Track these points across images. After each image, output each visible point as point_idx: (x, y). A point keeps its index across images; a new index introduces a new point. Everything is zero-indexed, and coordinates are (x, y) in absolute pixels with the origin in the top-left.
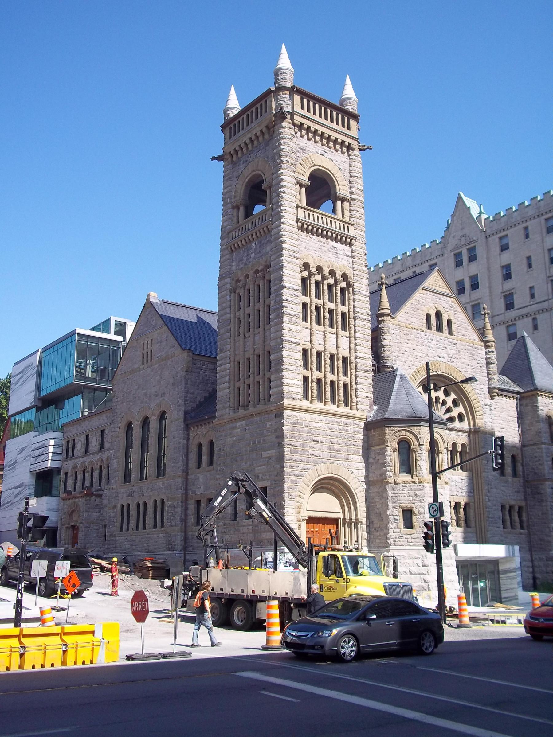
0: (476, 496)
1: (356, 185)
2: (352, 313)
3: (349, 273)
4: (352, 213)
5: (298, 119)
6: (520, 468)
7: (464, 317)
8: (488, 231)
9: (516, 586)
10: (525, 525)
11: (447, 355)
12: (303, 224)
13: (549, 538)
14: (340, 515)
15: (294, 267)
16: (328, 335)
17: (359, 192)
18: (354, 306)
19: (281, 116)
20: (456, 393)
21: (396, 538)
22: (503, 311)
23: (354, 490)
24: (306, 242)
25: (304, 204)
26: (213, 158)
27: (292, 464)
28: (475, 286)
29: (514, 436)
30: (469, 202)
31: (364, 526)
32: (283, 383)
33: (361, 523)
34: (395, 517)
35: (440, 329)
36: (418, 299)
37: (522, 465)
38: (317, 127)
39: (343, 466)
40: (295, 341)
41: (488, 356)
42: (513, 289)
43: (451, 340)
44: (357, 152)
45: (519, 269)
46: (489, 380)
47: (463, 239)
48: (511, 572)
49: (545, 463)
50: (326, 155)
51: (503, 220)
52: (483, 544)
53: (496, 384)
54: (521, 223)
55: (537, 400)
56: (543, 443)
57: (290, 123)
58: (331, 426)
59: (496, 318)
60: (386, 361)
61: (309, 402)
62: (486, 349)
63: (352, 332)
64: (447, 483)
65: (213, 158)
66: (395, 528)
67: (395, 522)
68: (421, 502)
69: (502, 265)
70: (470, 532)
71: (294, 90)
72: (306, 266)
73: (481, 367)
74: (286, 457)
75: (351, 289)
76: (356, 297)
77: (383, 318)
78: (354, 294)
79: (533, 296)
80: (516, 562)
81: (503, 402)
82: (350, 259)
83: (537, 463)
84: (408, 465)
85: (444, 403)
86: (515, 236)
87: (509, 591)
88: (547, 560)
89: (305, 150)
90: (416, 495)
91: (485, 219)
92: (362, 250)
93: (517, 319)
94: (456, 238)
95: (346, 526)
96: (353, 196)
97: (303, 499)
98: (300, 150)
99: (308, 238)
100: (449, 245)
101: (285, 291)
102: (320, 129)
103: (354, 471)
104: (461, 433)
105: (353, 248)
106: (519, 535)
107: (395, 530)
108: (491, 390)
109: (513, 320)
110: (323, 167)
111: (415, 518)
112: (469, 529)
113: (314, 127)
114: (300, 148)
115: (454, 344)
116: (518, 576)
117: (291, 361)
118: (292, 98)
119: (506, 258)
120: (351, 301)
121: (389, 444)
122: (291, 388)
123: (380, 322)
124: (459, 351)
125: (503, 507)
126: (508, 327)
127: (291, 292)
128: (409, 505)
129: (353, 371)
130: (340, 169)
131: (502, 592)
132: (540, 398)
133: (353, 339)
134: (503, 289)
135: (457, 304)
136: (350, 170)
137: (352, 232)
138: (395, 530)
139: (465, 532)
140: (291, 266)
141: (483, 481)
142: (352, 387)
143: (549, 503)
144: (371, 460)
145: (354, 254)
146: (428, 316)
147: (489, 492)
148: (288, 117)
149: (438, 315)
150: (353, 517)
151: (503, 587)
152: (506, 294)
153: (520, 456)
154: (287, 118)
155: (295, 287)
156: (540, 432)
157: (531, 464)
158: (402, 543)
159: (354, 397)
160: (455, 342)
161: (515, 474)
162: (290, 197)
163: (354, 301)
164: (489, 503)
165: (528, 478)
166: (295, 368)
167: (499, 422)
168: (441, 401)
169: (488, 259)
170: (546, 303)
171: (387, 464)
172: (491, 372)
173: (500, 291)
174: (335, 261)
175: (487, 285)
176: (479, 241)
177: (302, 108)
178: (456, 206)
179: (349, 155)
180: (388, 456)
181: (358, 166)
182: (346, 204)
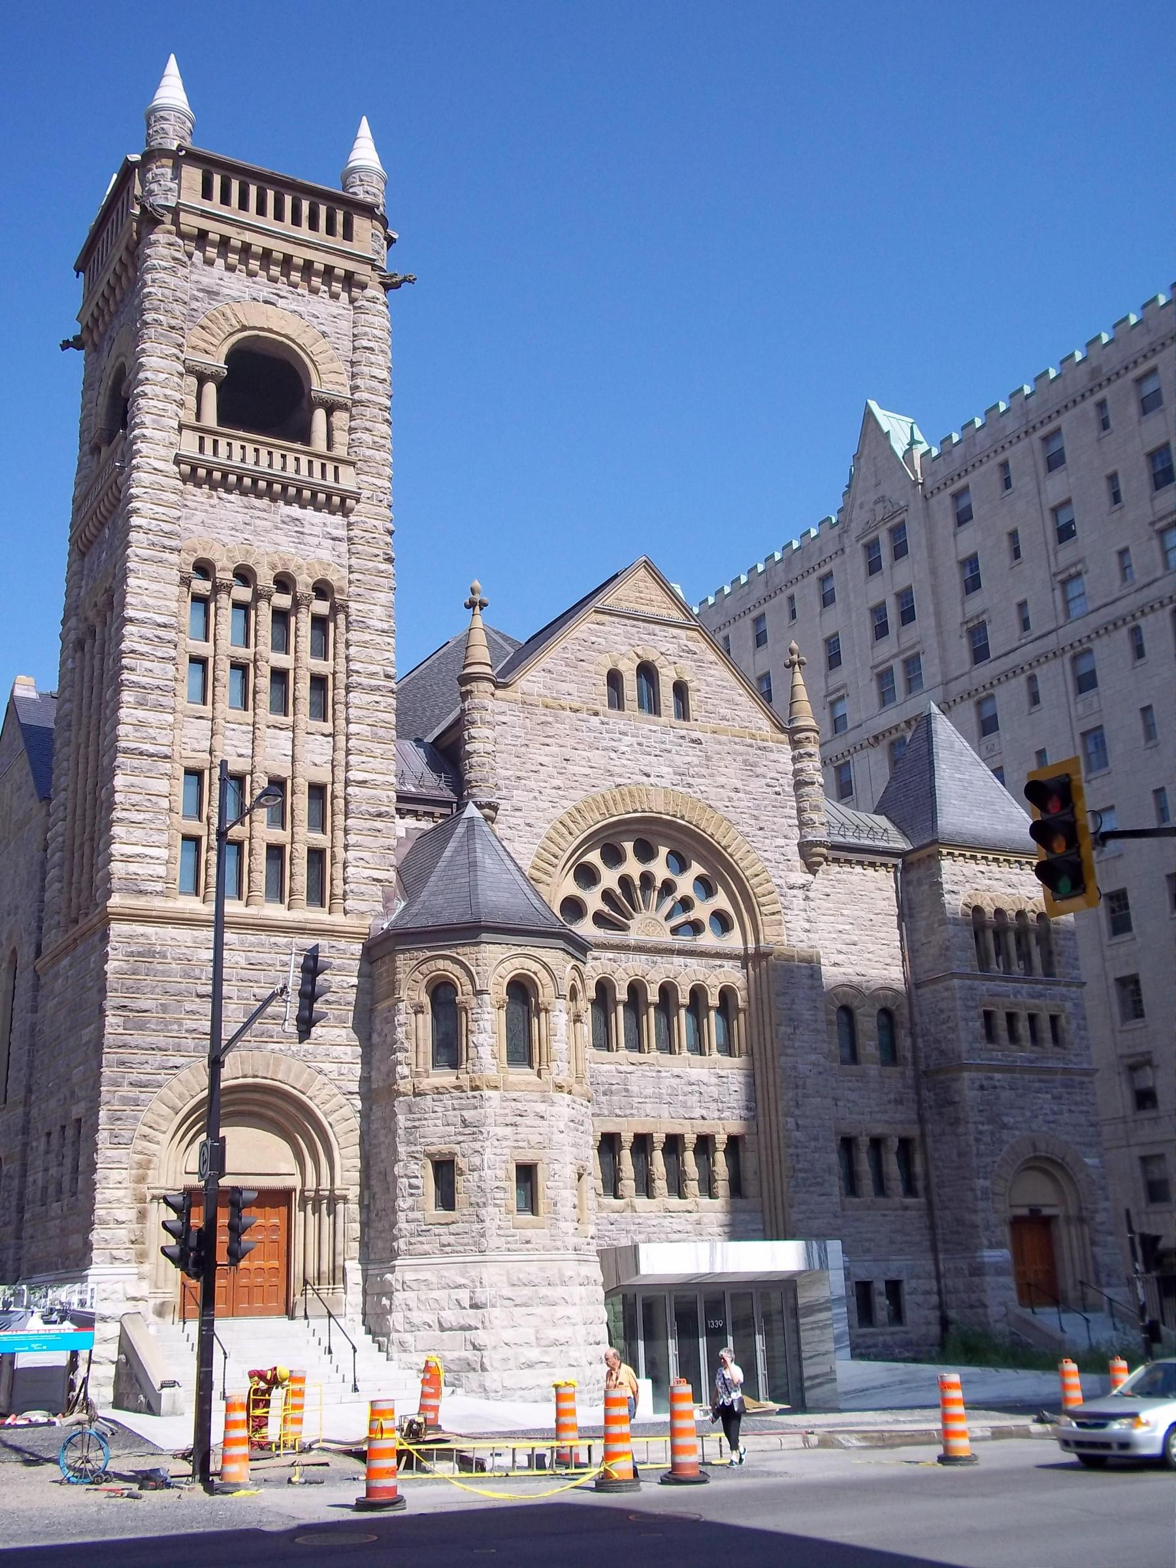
0: (761, 1118)
1: (366, 370)
2: (341, 677)
3: (335, 578)
4: (353, 436)
5: (190, 222)
6: (904, 1042)
7: (727, 675)
8: (929, 483)
9: (831, 1346)
10: (920, 1185)
11: (670, 770)
12: (194, 469)
13: (974, 1217)
14: (295, 1182)
15: (162, 571)
16: (265, 733)
17: (375, 384)
18: (348, 659)
19: (150, 220)
20: (703, 861)
21: (412, 1235)
22: (967, 667)
23: (326, 1115)
24: (206, 511)
25: (210, 418)
26: (66, 345)
27: (125, 1057)
28: (908, 616)
29: (889, 961)
30: (887, 420)
31: (354, 1208)
32: (111, 855)
33: (345, 1199)
34: (413, 1181)
35: (651, 705)
36: (584, 636)
37: (912, 1034)
38: (248, 237)
39: (293, 1056)
40: (152, 749)
41: (799, 766)
42: (983, 613)
43: (683, 732)
44: (375, 291)
45: (994, 563)
46: (802, 824)
47: (880, 505)
48: (820, 1311)
49: (961, 1024)
50: (281, 302)
51: (957, 452)
52: (778, 1239)
53: (819, 834)
54: (992, 455)
55: (940, 869)
56: (954, 975)
57: (169, 232)
58: (255, 957)
59: (952, 685)
60: (475, 790)
61: (200, 899)
62: (794, 749)
63: (341, 723)
64: (560, 1088)
65: (66, 345)
66: (412, 1209)
67: (412, 1195)
68: (475, 1140)
69: (961, 557)
70: (744, 1211)
71: (183, 158)
72: (204, 569)
73: (778, 794)
74: (109, 1039)
75: (341, 617)
76: (353, 636)
77: (468, 687)
78: (348, 630)
79: (1025, 624)
80: (835, 1283)
81: (854, 878)
82: (343, 547)
83: (944, 1027)
84: (449, 1048)
85: (668, 887)
86: (982, 484)
87: (816, 1360)
88: (971, 1275)
89: (217, 294)
90: (464, 1121)
91: (922, 456)
92: (376, 523)
93: (995, 682)
94: (866, 507)
95: (309, 1207)
96: (356, 396)
97: (158, 1143)
98: (201, 295)
99: (215, 501)
100: (853, 525)
101: (129, 629)
102: (259, 242)
103: (326, 1067)
104: (718, 962)
105: (352, 519)
106: (900, 1212)
107: (411, 1215)
108: (805, 848)
109: (988, 686)
110: (270, 330)
111: (460, 1182)
112: (740, 1203)
113: (238, 237)
114: (199, 290)
115: (693, 741)
116: (838, 1321)
117: (136, 798)
118: (177, 176)
119: (969, 540)
120: (341, 647)
121: (403, 994)
122: (133, 868)
123: (465, 696)
124: (708, 758)
125: (848, 1144)
126: (979, 704)
127: (148, 632)
128: (444, 1148)
129: (340, 819)
130: (324, 335)
131: (804, 1363)
132: (946, 864)
133: (341, 739)
134: (964, 614)
135: (704, 645)
136: (355, 335)
137: (348, 479)
138: (411, 1215)
139: (733, 1211)
140: (151, 568)
141: (778, 1080)
142: (333, 857)
143: (971, 1126)
144: (376, 1038)
145: (352, 533)
146: (614, 679)
147: (798, 1105)
148: (168, 218)
149: (647, 671)
150: (325, 1184)
151: (807, 1351)
152: (971, 625)
153: (906, 1011)
154: (163, 223)
155: (161, 619)
156: (947, 948)
157: (933, 1030)
158: (426, 1247)
159: (339, 882)
160: (696, 735)
161: (890, 1055)
162: (160, 405)
163: (348, 645)
164: (798, 1134)
165: (928, 1066)
166: (148, 816)
167: (841, 927)
168: (658, 884)
169: (931, 548)
170: (1053, 636)
171: (398, 1045)
172: (806, 805)
173: (960, 620)
174: (293, 551)
175: (931, 609)
176: (912, 509)
177: (207, 194)
178: (863, 435)
179: (352, 301)
180: (400, 1025)
181: (378, 320)
182: (340, 418)
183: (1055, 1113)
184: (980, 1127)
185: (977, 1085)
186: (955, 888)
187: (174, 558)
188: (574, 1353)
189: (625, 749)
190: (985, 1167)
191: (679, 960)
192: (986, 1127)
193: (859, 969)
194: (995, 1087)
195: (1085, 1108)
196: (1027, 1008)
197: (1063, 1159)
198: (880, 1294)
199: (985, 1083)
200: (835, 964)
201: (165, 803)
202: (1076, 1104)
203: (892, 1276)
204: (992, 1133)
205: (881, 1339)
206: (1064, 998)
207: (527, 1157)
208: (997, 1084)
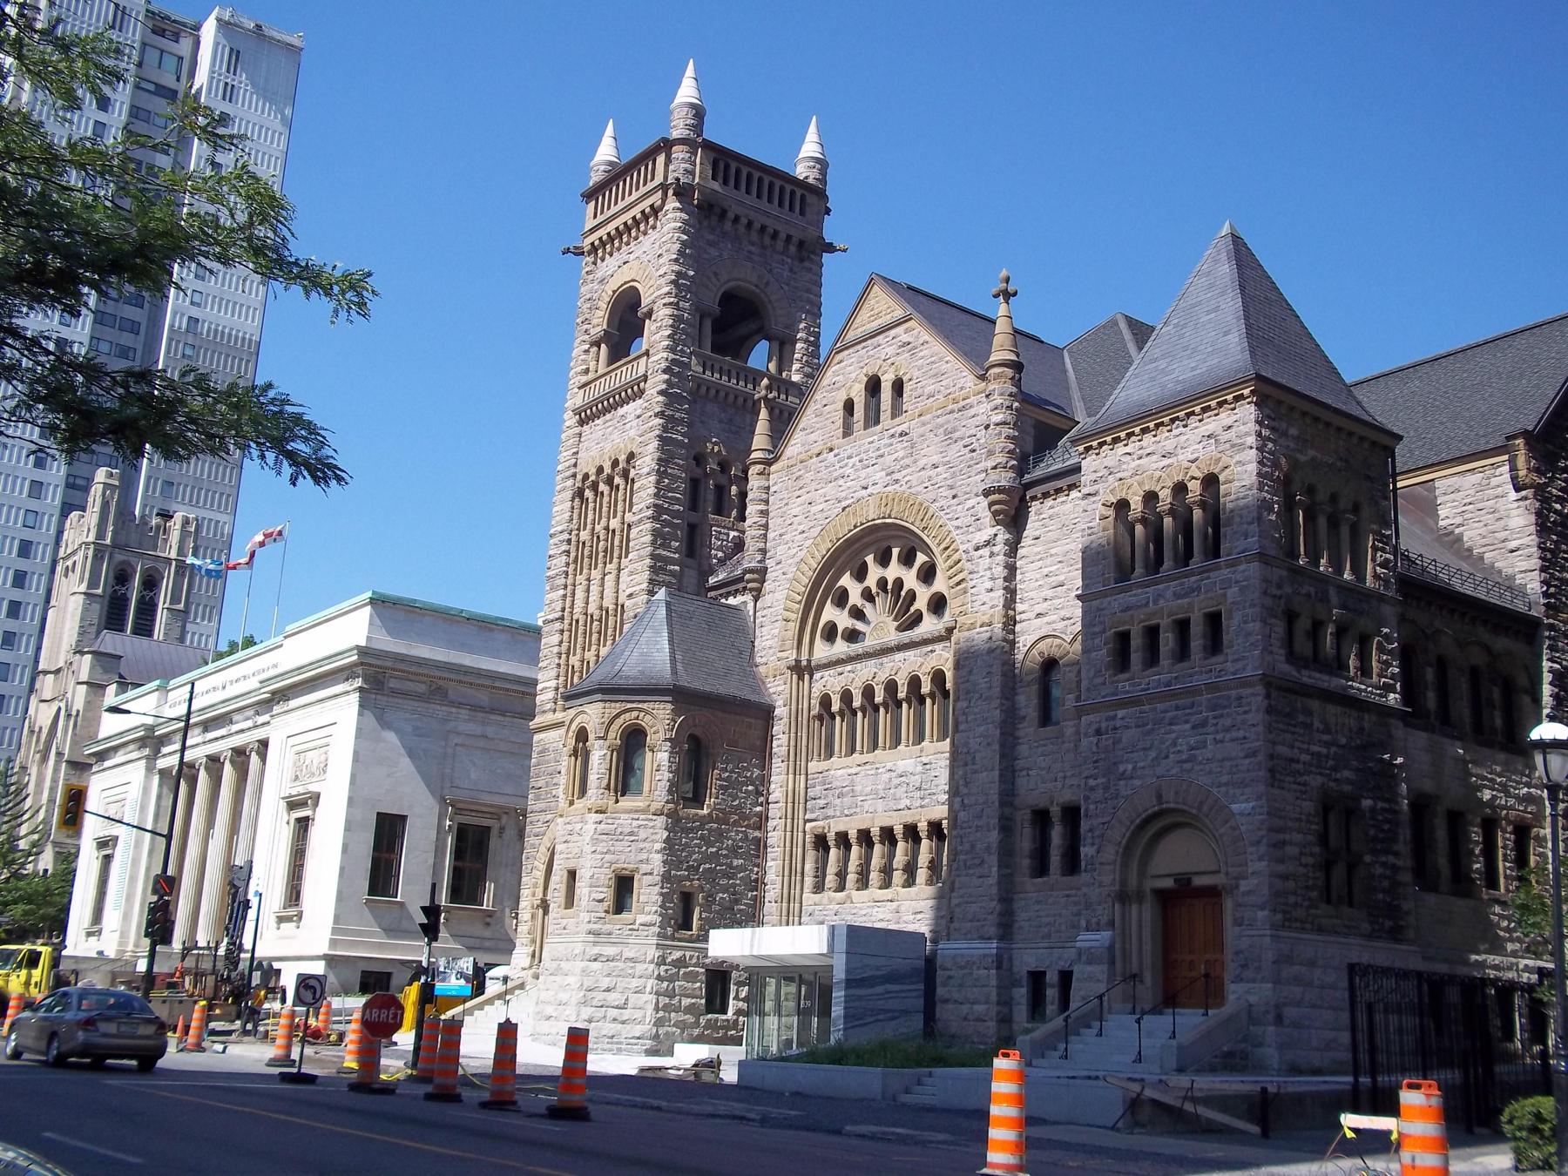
167: (1046, 571)
184: (1092, 782)
185: (1095, 726)
187: (570, 482)
189: (848, 471)
191: (899, 656)
195: (1241, 734)
198: (1052, 986)
201: (556, 650)
202: (1227, 730)
204: (1106, 788)
206: (1227, 583)
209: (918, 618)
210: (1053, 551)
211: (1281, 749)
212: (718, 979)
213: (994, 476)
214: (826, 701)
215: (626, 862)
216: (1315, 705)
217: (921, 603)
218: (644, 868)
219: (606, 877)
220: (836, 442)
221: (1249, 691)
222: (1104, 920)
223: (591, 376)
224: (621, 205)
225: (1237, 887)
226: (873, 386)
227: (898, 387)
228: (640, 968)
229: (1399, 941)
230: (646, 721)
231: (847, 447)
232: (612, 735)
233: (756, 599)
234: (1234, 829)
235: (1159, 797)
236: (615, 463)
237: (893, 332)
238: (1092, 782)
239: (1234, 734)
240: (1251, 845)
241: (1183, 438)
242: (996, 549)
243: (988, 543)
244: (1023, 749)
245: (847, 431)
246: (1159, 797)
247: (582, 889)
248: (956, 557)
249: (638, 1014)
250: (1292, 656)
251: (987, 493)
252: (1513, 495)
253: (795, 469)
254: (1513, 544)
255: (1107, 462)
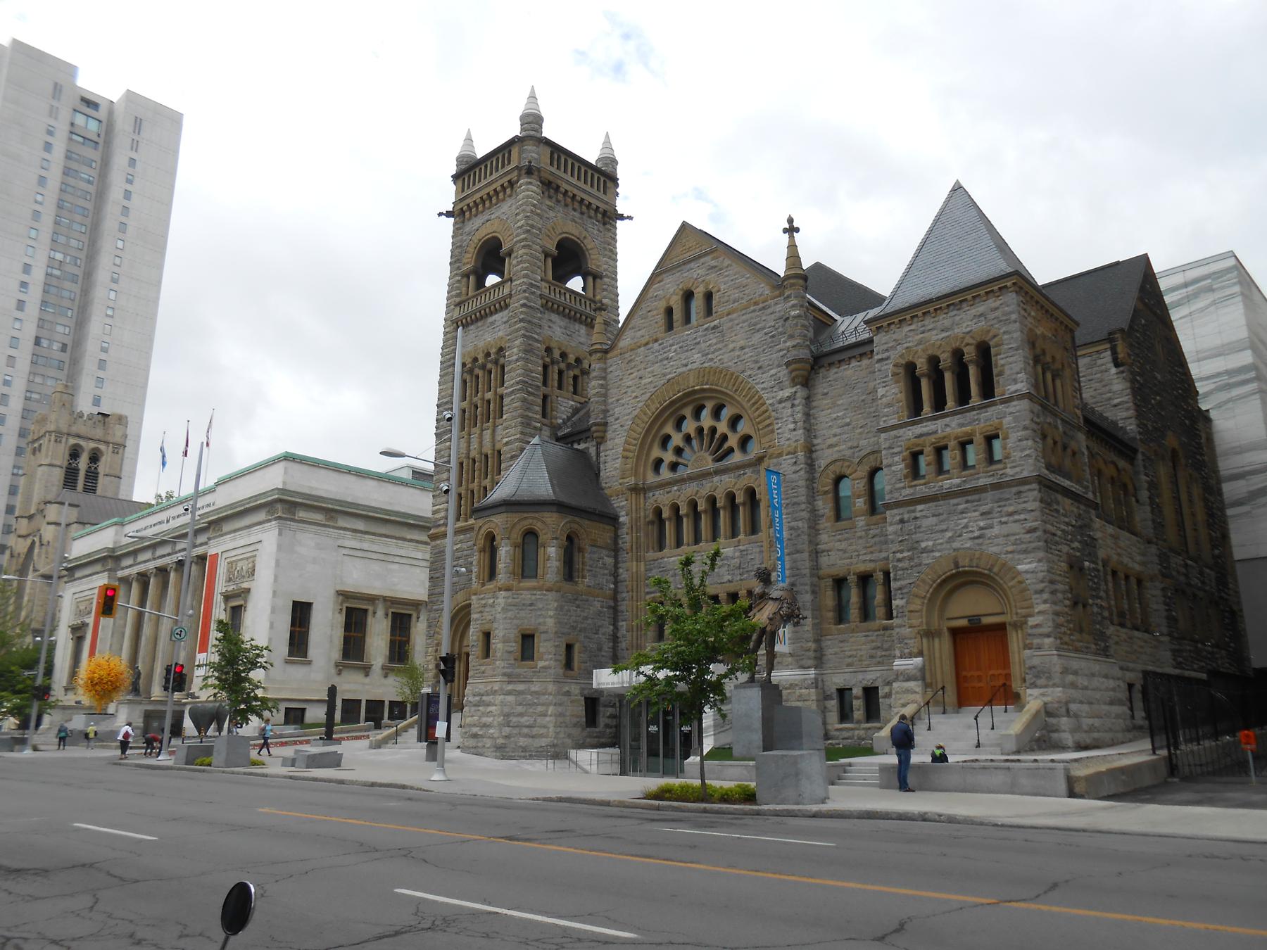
81: (849, 372)
183: (981, 529)
184: (899, 556)
185: (898, 518)
186: (884, 356)
188: (491, 731)
190: (900, 589)
191: (716, 479)
192: (905, 554)
193: (850, 444)
194: (916, 518)
195: (1022, 517)
196: (956, 438)
197: (990, 570)
198: (857, 698)
199: (906, 517)
200: (831, 446)
202: (1011, 514)
203: (865, 683)
205: (856, 732)
207: (486, 628)
208: (918, 515)
209: (731, 450)
210: (840, 402)
211: (1049, 527)
212: (592, 703)
213: (794, 352)
214: (658, 512)
215: (529, 623)
216: (1060, 497)
217: (733, 441)
218: (542, 628)
219: (514, 634)
220: (659, 335)
221: (1027, 487)
222: (915, 650)
223: (464, 298)
224: (484, 183)
225: (1026, 623)
226: (688, 296)
227: (709, 296)
228: (544, 698)
229: (1107, 656)
230: (538, 526)
231: (670, 339)
232: (514, 535)
233: (598, 445)
234: (1020, 582)
235: (957, 566)
236: (488, 355)
237: (702, 260)
238: (899, 556)
239: (1017, 517)
240: (1036, 592)
241: (957, 318)
242: (796, 402)
243: (789, 398)
244: (824, 537)
245: (670, 326)
246: (957, 566)
247: (497, 644)
248: (764, 408)
249: (542, 731)
250: (1049, 467)
251: (788, 364)
252: (1114, 370)
253: (627, 355)
254: (1116, 401)
255: (895, 336)
